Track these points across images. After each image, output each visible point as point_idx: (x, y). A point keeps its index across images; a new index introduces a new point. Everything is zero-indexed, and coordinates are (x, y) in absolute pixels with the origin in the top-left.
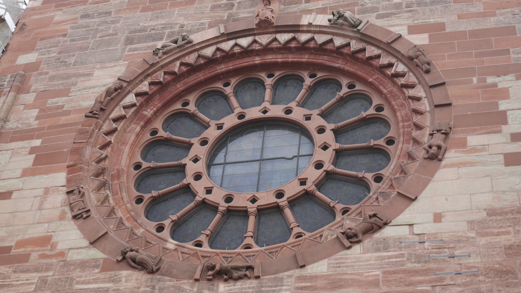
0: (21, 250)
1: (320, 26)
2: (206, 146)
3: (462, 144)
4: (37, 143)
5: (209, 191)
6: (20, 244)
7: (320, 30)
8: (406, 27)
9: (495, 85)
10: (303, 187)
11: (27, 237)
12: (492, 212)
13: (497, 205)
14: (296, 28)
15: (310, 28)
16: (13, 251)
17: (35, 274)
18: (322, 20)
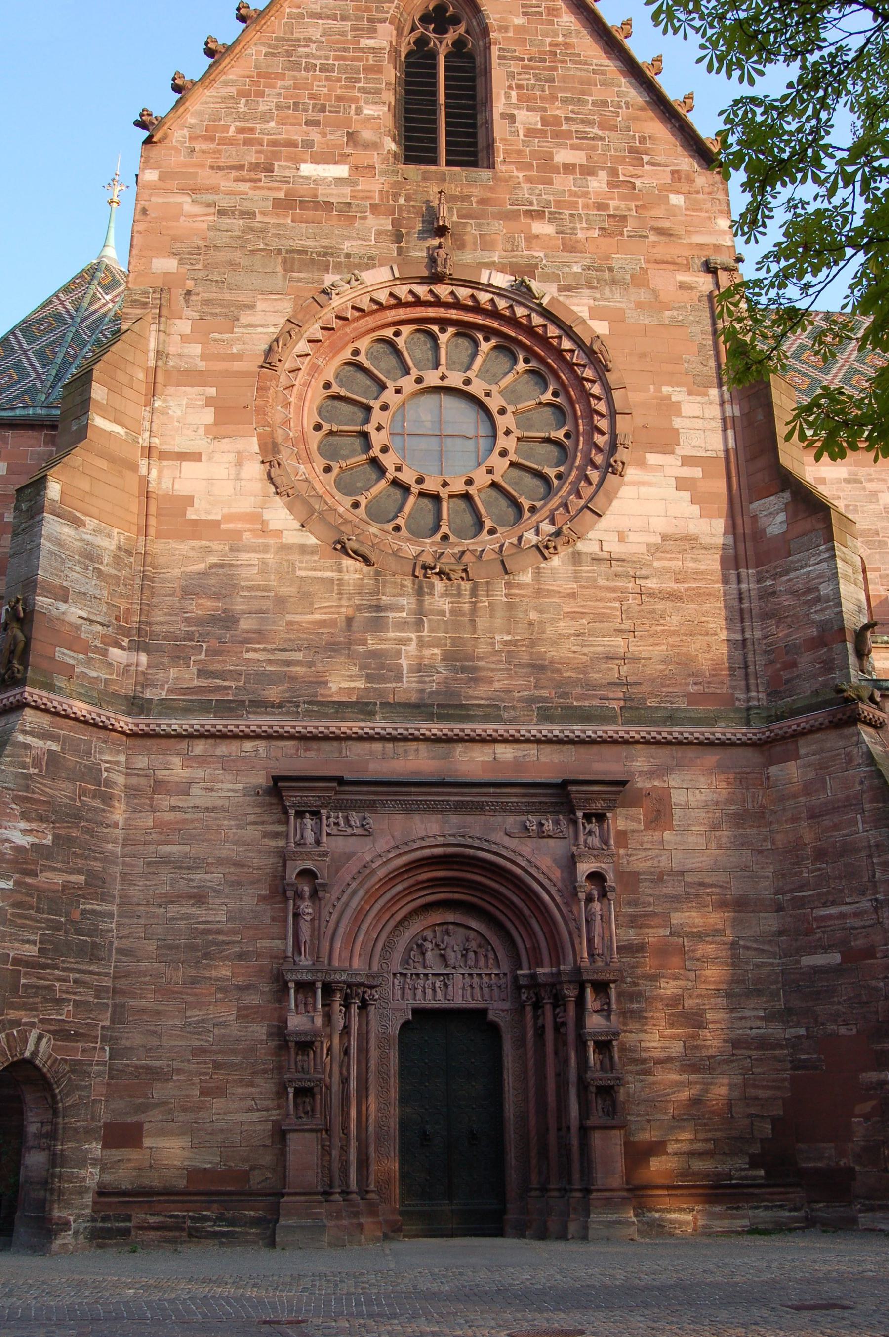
0: (231, 526)
1: (500, 289)
2: (387, 413)
3: (642, 464)
4: (212, 391)
5: (398, 469)
6: (229, 518)
7: (500, 292)
8: (586, 309)
9: (669, 397)
10: (490, 476)
11: (233, 510)
12: (665, 538)
13: (670, 530)
14: (475, 285)
15: (489, 287)
16: (224, 526)
17: (253, 555)
18: (502, 280)
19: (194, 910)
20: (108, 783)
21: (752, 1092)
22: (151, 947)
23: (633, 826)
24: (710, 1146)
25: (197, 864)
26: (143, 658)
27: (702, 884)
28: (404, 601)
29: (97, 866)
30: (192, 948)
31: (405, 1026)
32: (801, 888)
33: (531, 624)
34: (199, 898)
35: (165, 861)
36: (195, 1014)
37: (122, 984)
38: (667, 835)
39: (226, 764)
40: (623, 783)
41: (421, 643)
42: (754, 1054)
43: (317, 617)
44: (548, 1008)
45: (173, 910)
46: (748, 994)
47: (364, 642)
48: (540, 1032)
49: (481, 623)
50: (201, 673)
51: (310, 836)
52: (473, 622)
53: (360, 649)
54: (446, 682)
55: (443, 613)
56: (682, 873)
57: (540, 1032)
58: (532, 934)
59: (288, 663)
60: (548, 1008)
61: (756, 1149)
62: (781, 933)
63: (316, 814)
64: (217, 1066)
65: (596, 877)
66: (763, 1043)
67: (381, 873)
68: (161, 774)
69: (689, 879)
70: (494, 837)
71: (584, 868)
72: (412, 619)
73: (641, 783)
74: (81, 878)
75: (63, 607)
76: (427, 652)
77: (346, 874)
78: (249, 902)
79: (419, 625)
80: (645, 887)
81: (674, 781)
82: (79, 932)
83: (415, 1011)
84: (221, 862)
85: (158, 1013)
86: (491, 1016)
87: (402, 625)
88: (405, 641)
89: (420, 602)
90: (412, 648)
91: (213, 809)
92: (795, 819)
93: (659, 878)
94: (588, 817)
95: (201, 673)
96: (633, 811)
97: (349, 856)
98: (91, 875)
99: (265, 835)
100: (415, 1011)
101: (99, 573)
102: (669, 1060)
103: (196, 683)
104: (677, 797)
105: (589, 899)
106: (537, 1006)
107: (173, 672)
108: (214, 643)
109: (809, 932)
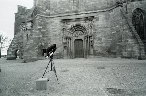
19: (56, 32)
20: (47, 22)
21: (106, 45)
22: (52, 36)
23: (95, 21)
24: (102, 50)
25: (55, 28)
26: (49, 11)
27: (102, 26)
28: (72, 2)
29: (47, 29)
30: (55, 36)
31: (75, 41)
32: (112, 25)
33: (84, 2)
34: (56, 31)
35: (53, 28)
36: (56, 41)
37: (50, 39)
38: (98, 21)
39: (57, 19)
40: (94, 17)
41: (74, 6)
42: (107, 42)
43: (64, 5)
44: (87, 39)
45: (54, 33)
46: (106, 36)
47: (68, 6)
48: (86, 41)
49: (79, 3)
50: (54, 12)
51: (64, 25)
52: (79, 3)
53: (68, 7)
54: (76, 9)
55: (76, 2)
56: (100, 25)
57: (86, 41)
58: (85, 32)
59: (62, 9)
60: (87, 39)
61: (107, 51)
62: (110, 30)
63: (65, 23)
64: (58, 45)
65: (91, 26)
66: (108, 41)
67: (71, 28)
68: (52, 21)
69: (101, 25)
70: (81, 23)
71: (89, 25)
72: (73, 3)
73: (96, 17)
74: (45, 30)
75: (41, 7)
76: (74, 6)
77: (68, 28)
78: (60, 31)
79: (73, 4)
80: (96, 27)
81: (99, 16)
82: (46, 35)
83: (75, 40)
84: (57, 28)
85: (53, 41)
86: (82, 40)
87: (72, 4)
88: (72, 6)
89: (73, 2)
90: (73, 6)
91: (56, 23)
92: (112, 18)
93: (97, 25)
94: (90, 20)
95: (54, 12)
96: (95, 19)
97: (68, 26)
98: (46, 30)
99: (61, 25)
100: (75, 40)
101: (44, 4)
102: (98, 43)
103: (54, 12)
104: (99, 17)
105: (90, 28)
106: (86, 39)
107: (52, 12)
108: (55, 9)
109: (113, 29)
